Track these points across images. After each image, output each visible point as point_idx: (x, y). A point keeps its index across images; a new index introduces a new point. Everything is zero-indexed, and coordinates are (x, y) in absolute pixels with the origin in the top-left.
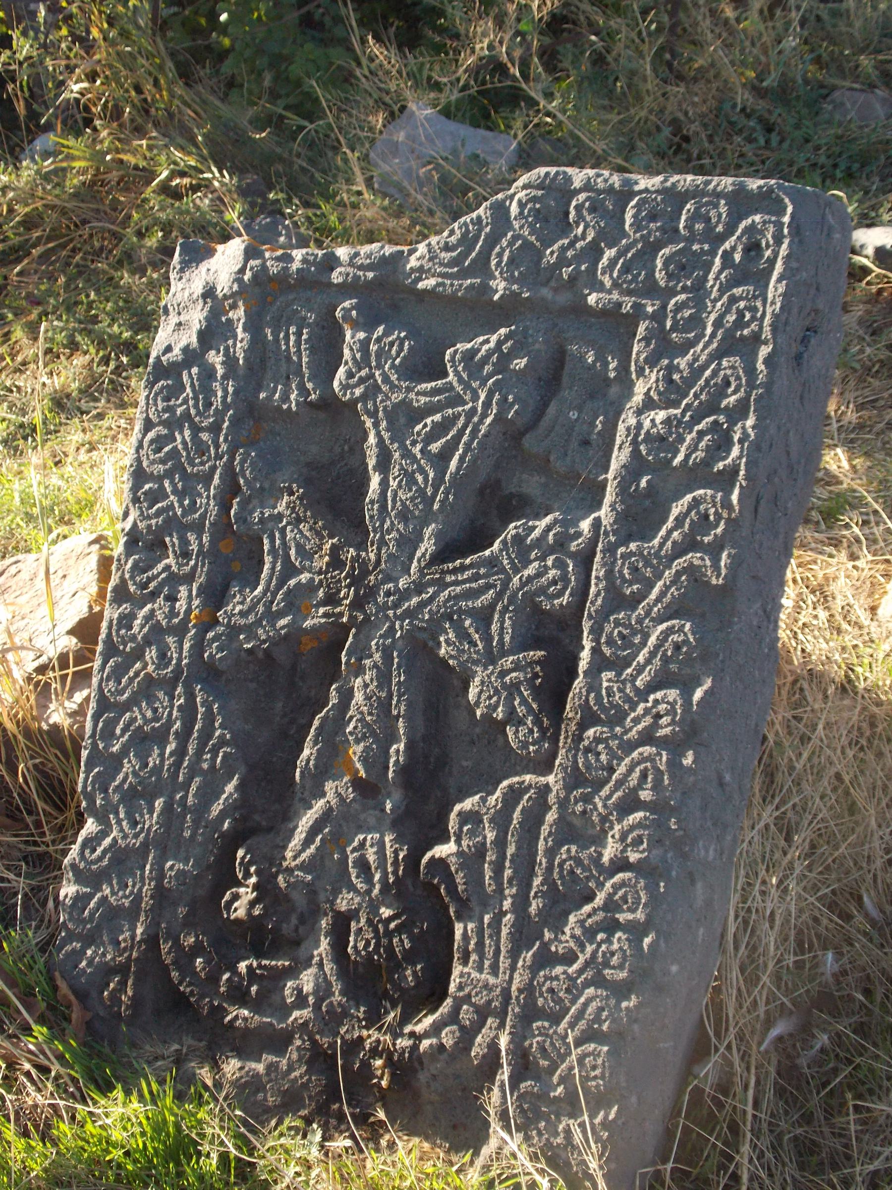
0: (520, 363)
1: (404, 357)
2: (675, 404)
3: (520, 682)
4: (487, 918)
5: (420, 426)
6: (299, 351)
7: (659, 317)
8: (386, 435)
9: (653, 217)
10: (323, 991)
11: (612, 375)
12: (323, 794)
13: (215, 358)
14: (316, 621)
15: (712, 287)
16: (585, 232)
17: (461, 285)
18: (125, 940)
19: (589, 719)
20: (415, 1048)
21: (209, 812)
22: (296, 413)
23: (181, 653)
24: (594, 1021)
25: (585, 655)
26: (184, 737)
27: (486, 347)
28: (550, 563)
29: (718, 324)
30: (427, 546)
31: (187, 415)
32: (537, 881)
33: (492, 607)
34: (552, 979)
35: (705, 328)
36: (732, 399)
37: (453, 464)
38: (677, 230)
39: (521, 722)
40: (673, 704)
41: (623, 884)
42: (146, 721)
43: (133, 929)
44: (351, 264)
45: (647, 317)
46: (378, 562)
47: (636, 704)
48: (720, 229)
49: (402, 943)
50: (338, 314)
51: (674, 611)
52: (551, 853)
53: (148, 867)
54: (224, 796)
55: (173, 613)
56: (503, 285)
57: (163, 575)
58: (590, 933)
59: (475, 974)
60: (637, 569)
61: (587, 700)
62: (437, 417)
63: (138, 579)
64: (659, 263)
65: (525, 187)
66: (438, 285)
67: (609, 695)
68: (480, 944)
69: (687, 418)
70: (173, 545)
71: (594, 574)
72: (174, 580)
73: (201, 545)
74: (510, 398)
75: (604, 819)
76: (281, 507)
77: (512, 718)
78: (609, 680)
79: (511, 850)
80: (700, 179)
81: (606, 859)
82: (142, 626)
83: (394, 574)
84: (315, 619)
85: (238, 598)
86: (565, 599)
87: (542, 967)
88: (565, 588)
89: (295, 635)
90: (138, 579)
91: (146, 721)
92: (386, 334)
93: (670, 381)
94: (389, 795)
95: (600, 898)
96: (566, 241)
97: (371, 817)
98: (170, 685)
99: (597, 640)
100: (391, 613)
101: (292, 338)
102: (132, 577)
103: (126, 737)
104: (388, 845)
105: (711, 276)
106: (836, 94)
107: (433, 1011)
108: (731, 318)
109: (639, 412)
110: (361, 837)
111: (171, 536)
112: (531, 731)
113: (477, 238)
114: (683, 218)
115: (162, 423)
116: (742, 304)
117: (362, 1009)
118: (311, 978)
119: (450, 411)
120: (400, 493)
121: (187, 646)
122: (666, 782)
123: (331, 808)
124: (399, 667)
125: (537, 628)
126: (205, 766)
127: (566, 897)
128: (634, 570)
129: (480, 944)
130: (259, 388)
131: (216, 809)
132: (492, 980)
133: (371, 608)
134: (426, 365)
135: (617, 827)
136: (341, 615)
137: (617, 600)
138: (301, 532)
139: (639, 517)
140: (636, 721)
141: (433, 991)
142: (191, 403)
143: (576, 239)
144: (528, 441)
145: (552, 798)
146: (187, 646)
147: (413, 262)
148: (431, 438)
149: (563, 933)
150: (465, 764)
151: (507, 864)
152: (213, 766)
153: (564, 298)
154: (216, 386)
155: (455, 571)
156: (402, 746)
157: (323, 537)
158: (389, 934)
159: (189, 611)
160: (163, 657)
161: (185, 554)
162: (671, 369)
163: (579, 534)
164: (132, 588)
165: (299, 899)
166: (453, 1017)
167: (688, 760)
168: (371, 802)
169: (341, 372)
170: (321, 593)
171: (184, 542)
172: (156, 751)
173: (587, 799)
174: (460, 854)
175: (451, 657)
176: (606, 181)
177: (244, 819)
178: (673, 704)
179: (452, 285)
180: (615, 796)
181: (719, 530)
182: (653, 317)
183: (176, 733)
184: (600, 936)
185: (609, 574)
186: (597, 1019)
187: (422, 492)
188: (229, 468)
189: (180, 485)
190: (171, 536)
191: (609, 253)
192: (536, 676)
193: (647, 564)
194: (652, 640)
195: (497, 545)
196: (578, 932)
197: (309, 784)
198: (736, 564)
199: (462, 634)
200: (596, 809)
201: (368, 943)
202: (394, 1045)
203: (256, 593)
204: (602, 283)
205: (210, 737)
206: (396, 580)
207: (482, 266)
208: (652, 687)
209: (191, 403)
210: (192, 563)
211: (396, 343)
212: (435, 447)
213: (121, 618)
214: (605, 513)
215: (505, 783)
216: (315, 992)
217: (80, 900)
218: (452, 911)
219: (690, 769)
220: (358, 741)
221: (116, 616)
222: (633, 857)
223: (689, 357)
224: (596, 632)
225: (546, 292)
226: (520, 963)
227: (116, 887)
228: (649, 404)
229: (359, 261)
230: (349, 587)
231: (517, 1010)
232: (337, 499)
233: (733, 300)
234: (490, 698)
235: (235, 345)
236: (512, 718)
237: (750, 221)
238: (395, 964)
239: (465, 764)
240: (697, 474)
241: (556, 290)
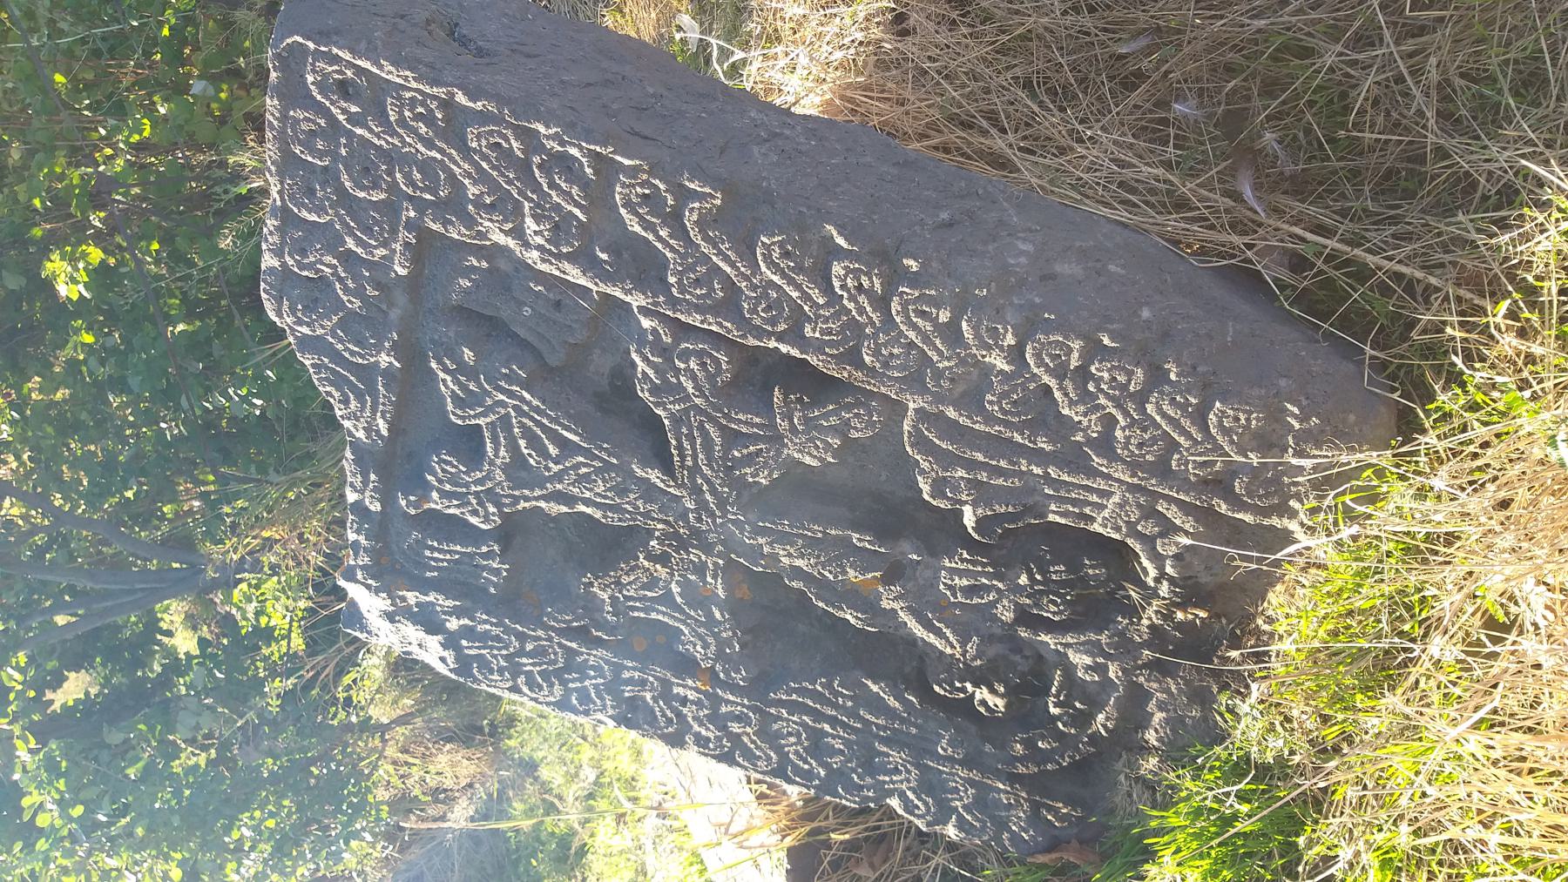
0: (468, 354)
2: (518, 207)
6: (450, 552)
8: (537, 492)
9: (311, 192)
10: (1094, 649)
11: (485, 264)
13: (453, 624)
15: (387, 142)
16: (328, 264)
20: (1171, 580)
25: (784, 348)
26: (818, 716)
27: (450, 384)
28: (682, 366)
29: (429, 144)
30: (654, 476)
32: (1018, 438)
33: (722, 428)
36: (515, 145)
38: (325, 168)
39: (847, 423)
41: (1038, 356)
42: (799, 742)
43: (999, 791)
44: (362, 492)
49: (1058, 571)
50: (413, 512)
51: (746, 249)
52: (989, 419)
55: (698, 703)
59: (1106, 513)
60: (697, 280)
62: (522, 443)
64: (362, 195)
65: (280, 315)
66: (383, 417)
67: (830, 334)
68: (1074, 502)
72: (665, 694)
73: (634, 669)
75: (962, 362)
78: (814, 330)
79: (980, 457)
82: (708, 729)
83: (680, 510)
87: (1114, 450)
89: (733, 607)
91: (799, 742)
92: (434, 474)
93: (492, 205)
94: (904, 554)
99: (770, 335)
101: (436, 555)
108: (423, 129)
109: (526, 245)
113: (333, 371)
115: (514, 678)
116: (407, 114)
124: (773, 523)
126: (850, 704)
127: (1040, 411)
128: (697, 282)
129: (1074, 502)
131: (892, 702)
132: (1116, 499)
133: (712, 537)
134: (469, 444)
135: (974, 351)
136: (715, 564)
137: (729, 306)
138: (630, 583)
139: (642, 267)
141: (1117, 555)
143: (335, 274)
144: (553, 361)
147: (361, 434)
148: (544, 454)
150: (883, 478)
152: (851, 698)
153: (401, 298)
155: (682, 457)
159: (697, 690)
160: (739, 718)
161: (643, 683)
162: (478, 203)
163: (654, 331)
166: (1149, 541)
168: (908, 571)
169: (474, 520)
170: (693, 577)
171: (630, 681)
173: (938, 375)
175: (770, 475)
178: (848, 271)
181: (662, 187)
185: (699, 309)
186: (1182, 407)
187: (597, 471)
188: (560, 632)
191: (351, 243)
192: (800, 400)
193: (692, 268)
196: (1081, 409)
198: (699, 174)
199: (749, 460)
200: (951, 368)
201: (1054, 603)
204: (383, 257)
207: (367, 373)
208: (828, 289)
211: (442, 466)
212: (553, 451)
214: (636, 301)
216: (1093, 655)
217: (961, 825)
219: (922, 265)
220: (845, 573)
222: (1010, 340)
223: (466, 182)
224: (760, 333)
225: (395, 314)
228: (518, 233)
229: (359, 485)
230: (688, 553)
233: (402, 121)
234: (817, 447)
240: (598, 196)
241: (391, 305)
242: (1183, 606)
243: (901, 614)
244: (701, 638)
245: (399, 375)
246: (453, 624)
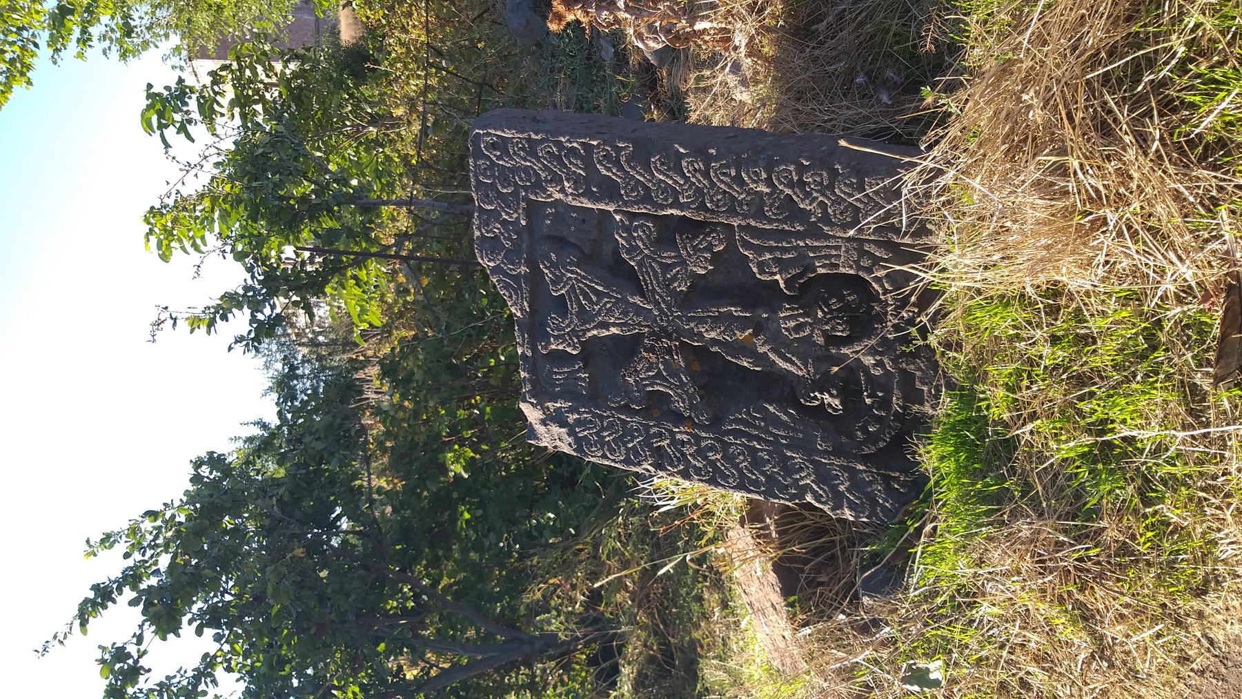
7: (525, 188)
10: (872, 351)
13: (572, 418)
16: (497, 228)
19: (702, 207)
29: (525, 159)
30: (637, 300)
31: (597, 434)
33: (660, 264)
41: (778, 179)
52: (770, 221)
55: (689, 442)
68: (826, 257)
72: (674, 442)
75: (748, 194)
76: (631, 380)
79: (773, 243)
81: (768, 190)
89: (689, 371)
95: (788, 191)
98: (726, 445)
121: (703, 435)
127: (791, 211)
128: (632, 190)
129: (826, 257)
131: (784, 418)
134: (560, 305)
137: (647, 198)
139: (609, 191)
140: (699, 181)
144: (586, 252)
145: (743, 223)
146: (703, 435)
147: (519, 314)
148: (591, 301)
153: (525, 237)
158: (831, 311)
161: (660, 435)
162: (546, 181)
173: (740, 203)
185: (636, 203)
186: (851, 185)
199: (674, 278)
208: (683, 176)
211: (553, 319)
214: (611, 208)
216: (873, 355)
217: (852, 506)
222: (764, 176)
224: (663, 207)
225: (524, 246)
228: (562, 191)
232: (626, 349)
233: (515, 153)
238: (846, 307)
240: (589, 165)
241: (522, 241)
246: (572, 418)
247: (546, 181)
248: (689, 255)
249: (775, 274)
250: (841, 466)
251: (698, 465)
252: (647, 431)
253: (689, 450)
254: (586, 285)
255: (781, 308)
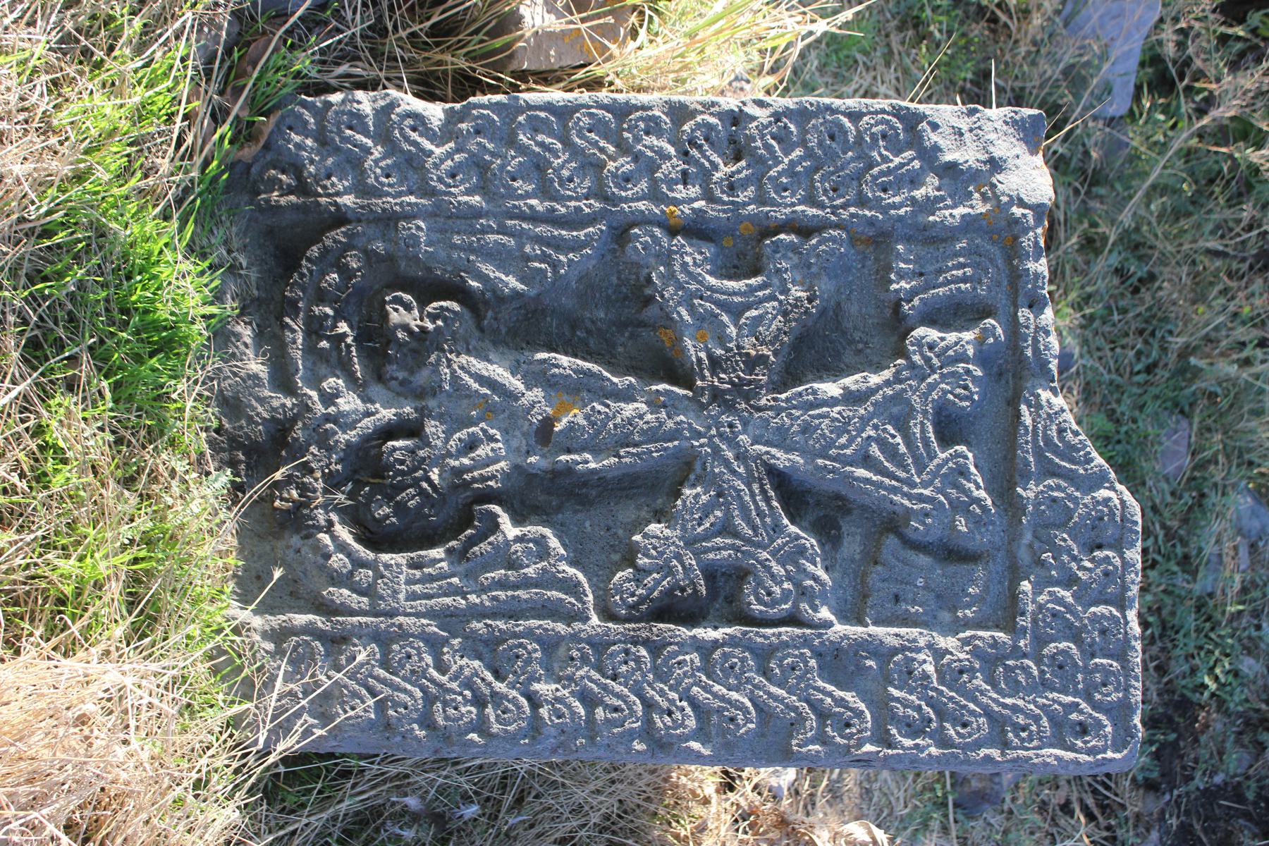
1: (954, 403)
2: (941, 681)
3: (674, 576)
4: (455, 580)
5: (893, 432)
7: (1017, 653)
8: (879, 397)
9: (1103, 632)
11: (960, 614)
12: (529, 388)
13: (929, 188)
14: (692, 351)
15: (1046, 698)
16: (1086, 568)
17: (1027, 452)
18: (333, 185)
19: (655, 649)
21: (485, 261)
22: (888, 290)
23: (632, 200)
24: (393, 701)
26: (551, 218)
28: (786, 585)
29: (1015, 709)
30: (782, 459)
32: (501, 624)
33: (736, 534)
34: (419, 654)
35: (1010, 696)
36: (952, 732)
37: (861, 472)
38: (1093, 656)
39: (638, 581)
40: (683, 725)
41: (519, 707)
43: (347, 191)
45: (1015, 641)
46: (759, 409)
47: (677, 691)
48: (1098, 696)
52: (529, 633)
53: (413, 199)
54: (503, 277)
55: (671, 183)
56: (1031, 495)
57: (707, 164)
58: (468, 684)
59: (403, 577)
60: (793, 669)
61: (671, 644)
62: (903, 449)
63: (698, 133)
64: (1063, 645)
65: (1123, 502)
66: (1026, 428)
67: (679, 663)
68: (431, 578)
69: (931, 693)
70: (739, 172)
71: (783, 629)
72: (705, 176)
73: (745, 204)
74: (929, 521)
76: (797, 292)
77: (641, 572)
78: (692, 660)
79: (522, 593)
80: (1138, 670)
81: (536, 686)
82: (651, 148)
83: (750, 428)
84: (694, 350)
85: (698, 257)
86: (757, 607)
88: (765, 605)
90: (698, 133)
92: (975, 379)
93: (961, 672)
94: (543, 456)
95: (500, 687)
96: (1076, 553)
97: (518, 441)
98: (599, 192)
100: (714, 432)
102: (697, 125)
103: (537, 149)
104: (497, 467)
105: (1055, 695)
106: (1184, 423)
107: (358, 539)
108: (1021, 720)
110: (498, 437)
111: (748, 166)
112: (633, 595)
113: (1072, 461)
114: (1104, 661)
115: (859, 137)
116: (1034, 728)
117: (339, 467)
118: (353, 406)
119: (910, 461)
120: (827, 421)
121: (642, 205)
122: (615, 731)
123: (517, 399)
124: (666, 449)
125: (723, 574)
126: (528, 249)
129: (431, 578)
130: (908, 239)
131: (488, 269)
132: (402, 596)
133: (714, 410)
134: (950, 427)
135: (566, 692)
136: (703, 378)
137: (764, 655)
138: (775, 318)
139: (839, 663)
140: (662, 693)
141: (376, 538)
142: (884, 167)
144: (891, 541)
145: (577, 625)
146: (642, 205)
147: (1045, 395)
148: (882, 443)
149: (462, 657)
150: (587, 524)
151: (510, 593)
152: (528, 259)
153: (1024, 556)
154: (905, 193)
156: (592, 465)
157: (773, 345)
159: (676, 202)
161: (732, 188)
162: (972, 670)
163: (815, 609)
164: (686, 127)
165: (422, 377)
166: (359, 563)
167: (638, 746)
169: (933, 334)
170: (719, 352)
171: (744, 184)
172: (530, 188)
173: (584, 659)
174: (507, 543)
175: (684, 502)
176: (1133, 582)
177: (486, 303)
178: (683, 725)
179: (1027, 443)
180: (593, 686)
181: (838, 739)
182: (1015, 647)
183: (554, 210)
184: (467, 693)
185: (785, 645)
186: (396, 705)
187: (831, 444)
189: (799, 169)
190: (748, 166)
191: (1067, 595)
192: (683, 590)
193: (799, 678)
194: (734, 695)
195: (793, 529)
196: (467, 672)
197: (537, 368)
199: (707, 511)
201: (402, 462)
202: (316, 508)
203: (708, 277)
204: (1041, 593)
205: (558, 248)
206: (745, 432)
209: (884, 167)
210: (725, 198)
211: (967, 389)
212: (875, 450)
213: (655, 119)
214: (840, 629)
215: (581, 576)
216: (341, 414)
217: (357, 121)
218: (453, 543)
220: (587, 417)
221: (657, 113)
222: (544, 712)
224: (732, 641)
225: (1028, 537)
226: (425, 621)
227: (383, 164)
228: (939, 654)
230: (731, 382)
231: (383, 626)
232: (814, 349)
233: (1037, 719)
235: (947, 207)
236: (641, 572)
237: (1106, 722)
239: (587, 524)
240: (882, 707)
241: (1030, 546)
242: (299, 506)
243: (522, 387)
244: (689, 274)
245: (1017, 478)
246: (929, 188)
247: (972, 670)
248: (678, 557)
249: (520, 539)
250: (381, 194)
251: (652, 140)
252: (760, 187)
253: (671, 167)
254: (892, 476)
255: (506, 476)
